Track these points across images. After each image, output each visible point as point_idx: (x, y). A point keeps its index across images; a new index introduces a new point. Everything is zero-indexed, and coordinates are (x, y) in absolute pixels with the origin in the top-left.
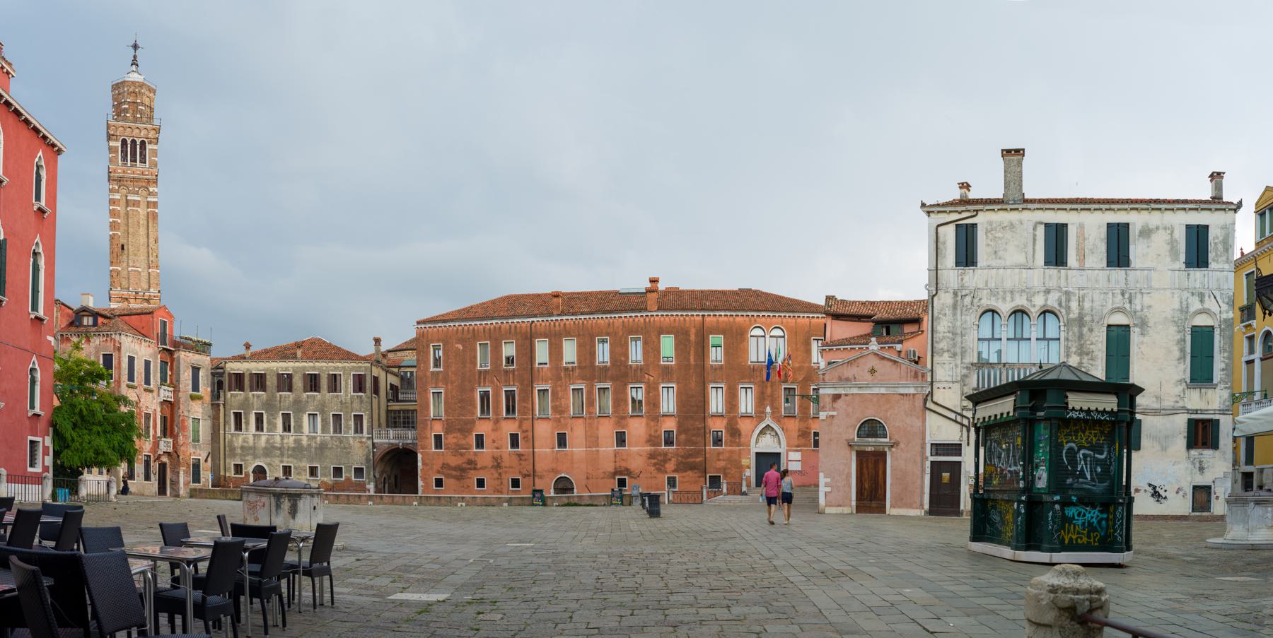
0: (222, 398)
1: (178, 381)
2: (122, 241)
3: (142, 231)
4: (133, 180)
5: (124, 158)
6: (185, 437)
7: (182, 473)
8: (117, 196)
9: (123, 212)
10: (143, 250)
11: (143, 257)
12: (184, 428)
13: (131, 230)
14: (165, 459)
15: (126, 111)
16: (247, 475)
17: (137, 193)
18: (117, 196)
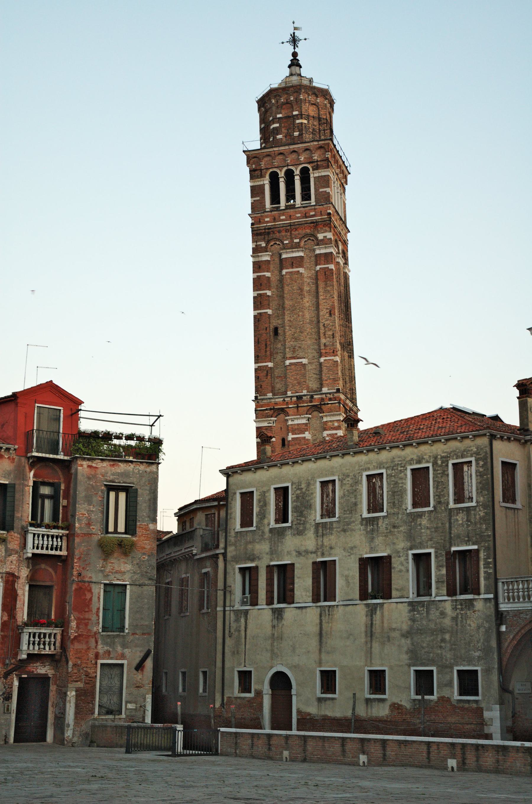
0: (222, 545)
1: (73, 516)
2: (275, 322)
3: (308, 301)
4: (291, 228)
5: (275, 199)
6: (83, 622)
7: (71, 694)
8: (265, 257)
9: (274, 280)
10: (309, 328)
11: (308, 342)
12: (84, 605)
13: (288, 303)
14: (42, 669)
15: (277, 131)
16: (259, 694)
17: (297, 246)
18: (265, 257)
